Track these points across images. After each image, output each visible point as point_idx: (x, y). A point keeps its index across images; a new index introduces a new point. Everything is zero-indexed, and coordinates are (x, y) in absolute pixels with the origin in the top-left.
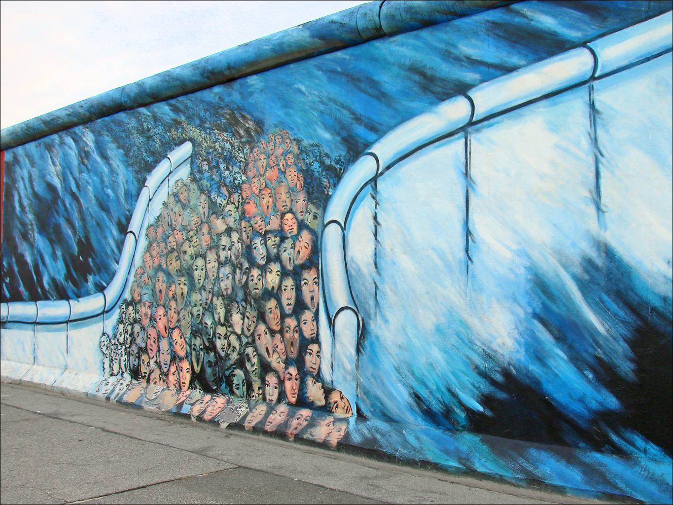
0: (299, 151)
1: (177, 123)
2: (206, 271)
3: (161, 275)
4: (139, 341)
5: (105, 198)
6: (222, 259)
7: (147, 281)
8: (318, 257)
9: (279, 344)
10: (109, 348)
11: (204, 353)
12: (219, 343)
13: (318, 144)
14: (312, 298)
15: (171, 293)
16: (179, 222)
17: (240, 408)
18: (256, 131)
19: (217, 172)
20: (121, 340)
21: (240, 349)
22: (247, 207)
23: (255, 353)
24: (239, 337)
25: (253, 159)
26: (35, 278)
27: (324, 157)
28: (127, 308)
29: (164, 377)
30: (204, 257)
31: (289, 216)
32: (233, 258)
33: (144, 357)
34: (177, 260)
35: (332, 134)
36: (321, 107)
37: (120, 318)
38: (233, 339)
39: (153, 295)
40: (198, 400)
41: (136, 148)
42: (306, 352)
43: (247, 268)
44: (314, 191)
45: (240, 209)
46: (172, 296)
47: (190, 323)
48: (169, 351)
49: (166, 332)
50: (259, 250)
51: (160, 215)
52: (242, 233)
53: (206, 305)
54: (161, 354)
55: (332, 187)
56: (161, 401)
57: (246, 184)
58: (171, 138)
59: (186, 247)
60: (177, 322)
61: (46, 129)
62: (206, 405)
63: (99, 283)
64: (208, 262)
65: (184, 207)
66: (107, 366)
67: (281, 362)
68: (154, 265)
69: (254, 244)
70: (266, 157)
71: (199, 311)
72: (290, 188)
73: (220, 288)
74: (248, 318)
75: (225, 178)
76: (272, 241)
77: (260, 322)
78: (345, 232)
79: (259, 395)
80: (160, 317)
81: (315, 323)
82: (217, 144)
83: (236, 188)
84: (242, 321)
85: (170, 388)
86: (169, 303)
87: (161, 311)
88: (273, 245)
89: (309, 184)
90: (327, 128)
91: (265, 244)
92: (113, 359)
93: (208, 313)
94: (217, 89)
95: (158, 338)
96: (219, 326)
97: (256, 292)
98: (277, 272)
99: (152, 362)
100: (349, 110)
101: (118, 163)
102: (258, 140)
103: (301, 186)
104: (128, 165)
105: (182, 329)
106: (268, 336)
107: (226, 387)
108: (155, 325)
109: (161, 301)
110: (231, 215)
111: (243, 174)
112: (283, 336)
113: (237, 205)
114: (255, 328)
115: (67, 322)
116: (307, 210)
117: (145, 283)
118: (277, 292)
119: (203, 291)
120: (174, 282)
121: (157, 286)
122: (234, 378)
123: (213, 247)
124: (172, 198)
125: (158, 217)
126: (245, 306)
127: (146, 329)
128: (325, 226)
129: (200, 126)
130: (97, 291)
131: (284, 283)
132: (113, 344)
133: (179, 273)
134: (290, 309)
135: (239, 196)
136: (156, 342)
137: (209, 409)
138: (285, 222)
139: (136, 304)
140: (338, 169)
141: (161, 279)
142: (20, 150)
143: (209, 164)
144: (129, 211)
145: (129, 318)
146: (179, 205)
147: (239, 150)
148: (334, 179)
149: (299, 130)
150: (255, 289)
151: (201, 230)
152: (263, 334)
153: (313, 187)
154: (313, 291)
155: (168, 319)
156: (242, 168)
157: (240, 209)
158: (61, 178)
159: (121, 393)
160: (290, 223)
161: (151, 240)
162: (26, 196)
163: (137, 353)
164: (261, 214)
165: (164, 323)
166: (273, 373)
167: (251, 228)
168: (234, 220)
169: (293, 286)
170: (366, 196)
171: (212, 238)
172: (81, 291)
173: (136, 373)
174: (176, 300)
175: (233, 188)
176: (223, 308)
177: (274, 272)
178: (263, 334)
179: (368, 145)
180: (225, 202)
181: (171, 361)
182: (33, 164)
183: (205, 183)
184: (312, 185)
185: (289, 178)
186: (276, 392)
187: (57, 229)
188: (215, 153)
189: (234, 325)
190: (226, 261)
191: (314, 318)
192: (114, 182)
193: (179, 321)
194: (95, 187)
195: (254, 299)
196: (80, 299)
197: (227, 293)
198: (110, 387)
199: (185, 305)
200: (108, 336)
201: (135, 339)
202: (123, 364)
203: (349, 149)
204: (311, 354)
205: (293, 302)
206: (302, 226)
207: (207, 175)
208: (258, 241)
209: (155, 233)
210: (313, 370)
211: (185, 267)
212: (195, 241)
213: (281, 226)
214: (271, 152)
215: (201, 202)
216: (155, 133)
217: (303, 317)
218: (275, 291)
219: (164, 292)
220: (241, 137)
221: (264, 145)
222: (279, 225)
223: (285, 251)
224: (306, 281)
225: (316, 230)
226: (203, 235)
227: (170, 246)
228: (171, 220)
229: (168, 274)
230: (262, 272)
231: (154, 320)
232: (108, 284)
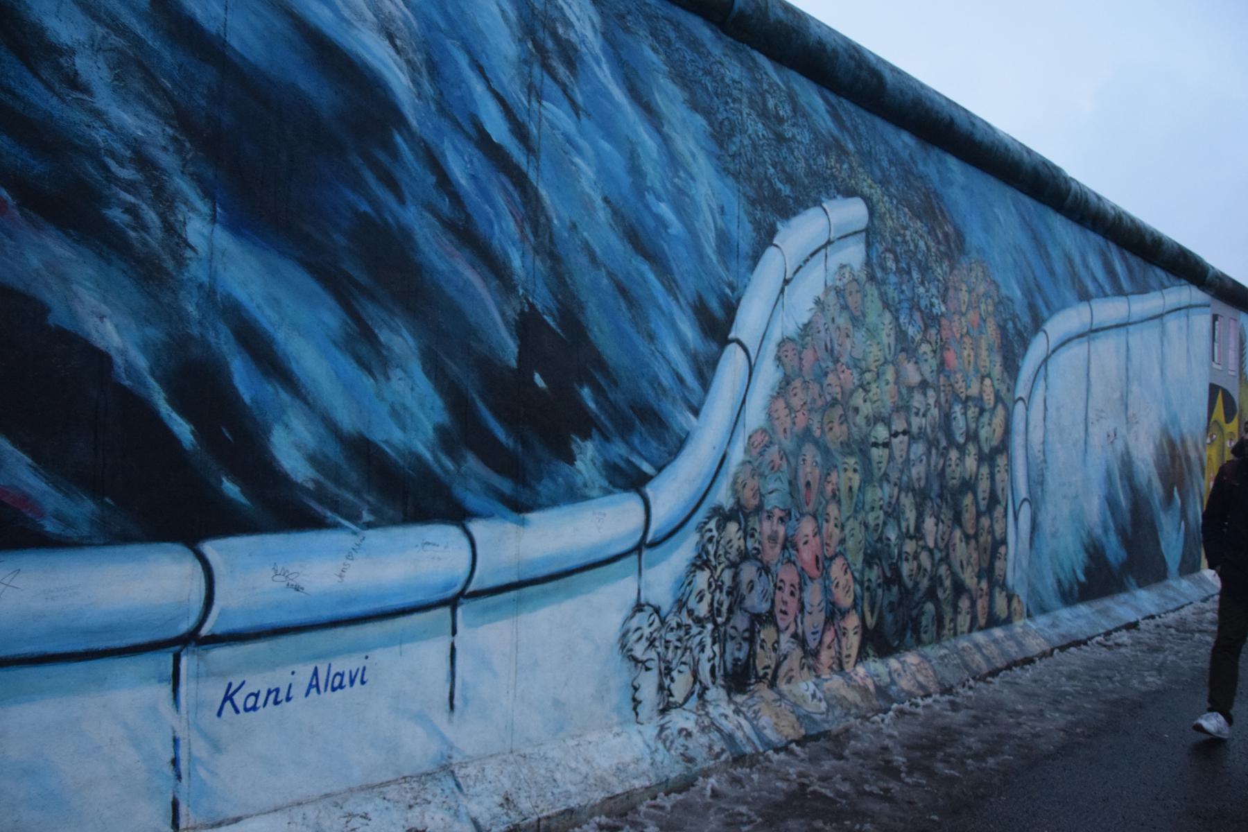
3: (809, 451)
6: (915, 429)
7: (778, 461)
10: (657, 644)
11: (883, 591)
12: (906, 568)
14: (1003, 490)
15: (829, 488)
19: (909, 281)
20: (703, 610)
24: (931, 552)
28: (721, 527)
32: (929, 431)
33: (767, 634)
34: (841, 424)
37: (699, 556)
38: (924, 558)
39: (791, 493)
43: (945, 448)
45: (938, 355)
46: (831, 494)
47: (863, 542)
48: (823, 604)
49: (818, 568)
51: (810, 322)
53: (889, 507)
54: (806, 615)
58: (829, 172)
59: (858, 399)
62: (908, 673)
63: (622, 464)
68: (796, 429)
71: (877, 518)
73: (910, 478)
74: (943, 522)
75: (919, 296)
77: (956, 526)
79: (950, 630)
82: (908, 233)
83: (931, 320)
84: (935, 528)
85: (823, 677)
86: (825, 508)
87: (807, 527)
90: (1018, 282)
92: (673, 665)
95: (800, 584)
96: (907, 541)
99: (785, 638)
100: (1033, 273)
101: (692, 145)
105: (849, 556)
106: (963, 544)
107: (911, 637)
108: (793, 558)
109: (807, 504)
110: (926, 360)
112: (977, 542)
115: (452, 603)
117: (773, 468)
119: (885, 485)
120: (836, 467)
121: (801, 474)
123: (902, 407)
124: (833, 293)
125: (806, 326)
127: (773, 569)
128: (1015, 402)
130: (615, 486)
132: (672, 629)
133: (847, 450)
135: (937, 334)
136: (797, 593)
139: (746, 516)
141: (809, 459)
143: (897, 260)
145: (726, 552)
146: (845, 314)
147: (937, 261)
151: (884, 374)
152: (958, 541)
155: (822, 541)
156: (942, 291)
161: (789, 371)
165: (814, 549)
167: (950, 388)
168: (930, 370)
171: (900, 393)
172: (540, 488)
178: (958, 541)
179: (1044, 321)
180: (918, 338)
181: (826, 623)
186: (968, 618)
188: (905, 247)
190: (919, 433)
193: (842, 541)
199: (855, 511)
200: (657, 610)
201: (743, 598)
205: (987, 495)
206: (998, 398)
208: (958, 409)
209: (796, 359)
211: (857, 437)
215: (884, 324)
216: (794, 136)
219: (815, 486)
227: (830, 394)
228: (831, 340)
229: (826, 451)
230: (960, 454)
232: (660, 469)
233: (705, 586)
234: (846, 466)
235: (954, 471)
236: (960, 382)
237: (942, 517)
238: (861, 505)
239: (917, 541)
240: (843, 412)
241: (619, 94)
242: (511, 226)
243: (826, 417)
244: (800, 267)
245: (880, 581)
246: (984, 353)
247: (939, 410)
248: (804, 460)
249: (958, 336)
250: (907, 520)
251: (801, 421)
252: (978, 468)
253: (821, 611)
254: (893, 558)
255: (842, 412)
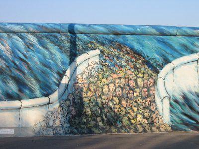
12: (116, 110)
24: (125, 108)
36: (156, 49)
38: (123, 109)
73: (116, 94)
90: (158, 54)
94: (111, 36)
220: (124, 52)
241: (41, 48)
242: (25, 67)
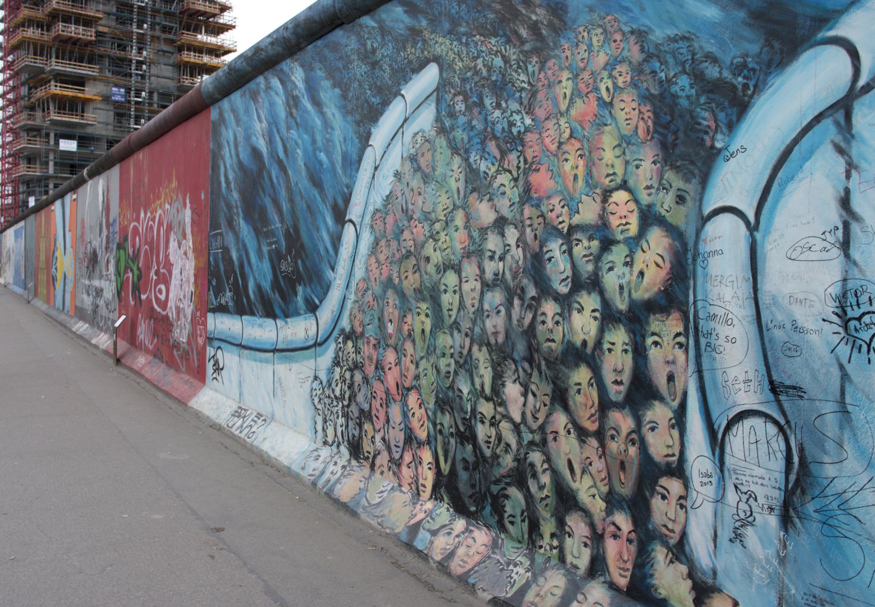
0: (643, 56)
1: (415, 33)
2: (461, 296)
4: (360, 398)
5: (318, 166)
6: (489, 276)
7: (372, 302)
8: (688, 289)
9: (595, 458)
11: (456, 443)
12: (482, 431)
13: (687, 35)
14: (671, 378)
15: (406, 328)
16: (419, 205)
17: (516, 565)
18: (551, 25)
19: (480, 113)
20: (338, 393)
21: (518, 450)
22: (534, 178)
23: (546, 466)
24: (516, 427)
25: (546, 82)
26: (240, 282)
27: (702, 62)
28: (345, 343)
29: (394, 467)
30: (458, 270)
31: (620, 196)
32: (508, 276)
33: (367, 426)
34: (415, 272)
35: (723, 8)
39: (379, 327)
40: (444, 526)
41: (356, 85)
42: (653, 492)
43: (533, 298)
44: (677, 142)
45: (521, 183)
46: (407, 333)
47: (435, 384)
48: (403, 426)
50: (558, 265)
51: (391, 193)
52: (525, 230)
54: (391, 429)
55: (724, 130)
56: (386, 512)
57: (532, 132)
60: (415, 378)
61: (249, 69)
62: (457, 540)
63: (310, 299)
64: (464, 280)
65: (426, 178)
66: (319, 427)
67: (597, 497)
69: (548, 251)
70: (570, 76)
71: (449, 365)
72: (622, 137)
73: (483, 330)
74: (534, 395)
75: (493, 124)
76: (584, 247)
77: (557, 406)
78: (758, 236)
79: (552, 548)
80: (389, 366)
81: (676, 433)
82: (480, 61)
84: (522, 399)
85: (403, 489)
86: (403, 344)
88: (585, 256)
89: (666, 126)
91: (570, 252)
92: (327, 418)
93: (463, 371)
96: (482, 400)
97: (550, 347)
98: (594, 311)
99: (378, 437)
102: (555, 43)
103: (648, 130)
104: (346, 112)
106: (573, 438)
107: (491, 514)
108: (382, 378)
110: (504, 193)
111: (527, 113)
112: (603, 445)
113: (515, 174)
114: (547, 417)
116: (660, 184)
117: (369, 307)
118: (593, 352)
119: (455, 332)
120: (410, 310)
121: (386, 314)
122: (506, 501)
123: (473, 252)
124: (408, 164)
125: (387, 197)
126: (529, 371)
129: (450, 32)
131: (609, 337)
133: (419, 296)
134: (620, 392)
135: (519, 157)
136: (384, 406)
137: (461, 551)
138: (611, 208)
139: (357, 338)
140: (740, 87)
142: (225, 104)
143: (466, 99)
144: (348, 187)
145: (347, 359)
146: (419, 175)
147: (519, 67)
148: (729, 112)
149: (643, 9)
150: (549, 340)
151: (452, 220)
152: (562, 432)
153: (675, 133)
154: (674, 362)
155: (401, 370)
156: (525, 102)
157: (521, 183)
158: (267, 139)
159: (334, 478)
160: (622, 210)
161: (378, 235)
162: (231, 166)
163: (357, 418)
164: (561, 192)
165: (396, 376)
166: (580, 513)
167: (541, 220)
168: (509, 204)
169: (627, 344)
170: (818, 147)
171: (471, 237)
173: (355, 449)
174: (414, 341)
175: (507, 142)
176: (490, 369)
177: (587, 312)
178: (562, 432)
180: (493, 169)
181: (405, 443)
182: (238, 121)
183: (460, 135)
184: (672, 127)
185: (621, 116)
187: (263, 212)
188: (476, 79)
189: (508, 403)
190: (494, 280)
191: (673, 421)
192: (328, 140)
193: (417, 377)
194: (305, 151)
195: (545, 359)
196: (289, 320)
197: (496, 340)
198: (319, 465)
199: (427, 353)
200: (321, 383)
201: (355, 395)
202: (339, 430)
203: (770, 36)
204: (664, 497)
205: (626, 377)
207: (462, 120)
208: (555, 247)
209: (382, 224)
210: (667, 532)
211: (428, 285)
212: (443, 240)
213: (602, 217)
214: (582, 65)
215: (453, 171)
216: (383, 56)
217: (649, 415)
218: (589, 350)
220: (523, 42)
221: (568, 53)
222: (599, 215)
223: (611, 269)
224: (656, 338)
225: (683, 227)
226: (456, 230)
227: (404, 247)
229: (402, 295)
230: (563, 309)
231: (382, 369)
232: (321, 302)
233: (338, 378)
234: (419, 310)
235: (551, 331)
236: (558, 209)
237: (533, 387)
238: (432, 349)
239: (494, 404)
240: (416, 263)
243: (402, 267)
244: (385, 152)
245: (453, 430)
246: (609, 155)
247: (524, 250)
248: (387, 302)
249: (553, 147)
250: (481, 376)
251: (385, 273)
252: (601, 331)
253: (401, 430)
254: (466, 413)
255: (415, 262)
